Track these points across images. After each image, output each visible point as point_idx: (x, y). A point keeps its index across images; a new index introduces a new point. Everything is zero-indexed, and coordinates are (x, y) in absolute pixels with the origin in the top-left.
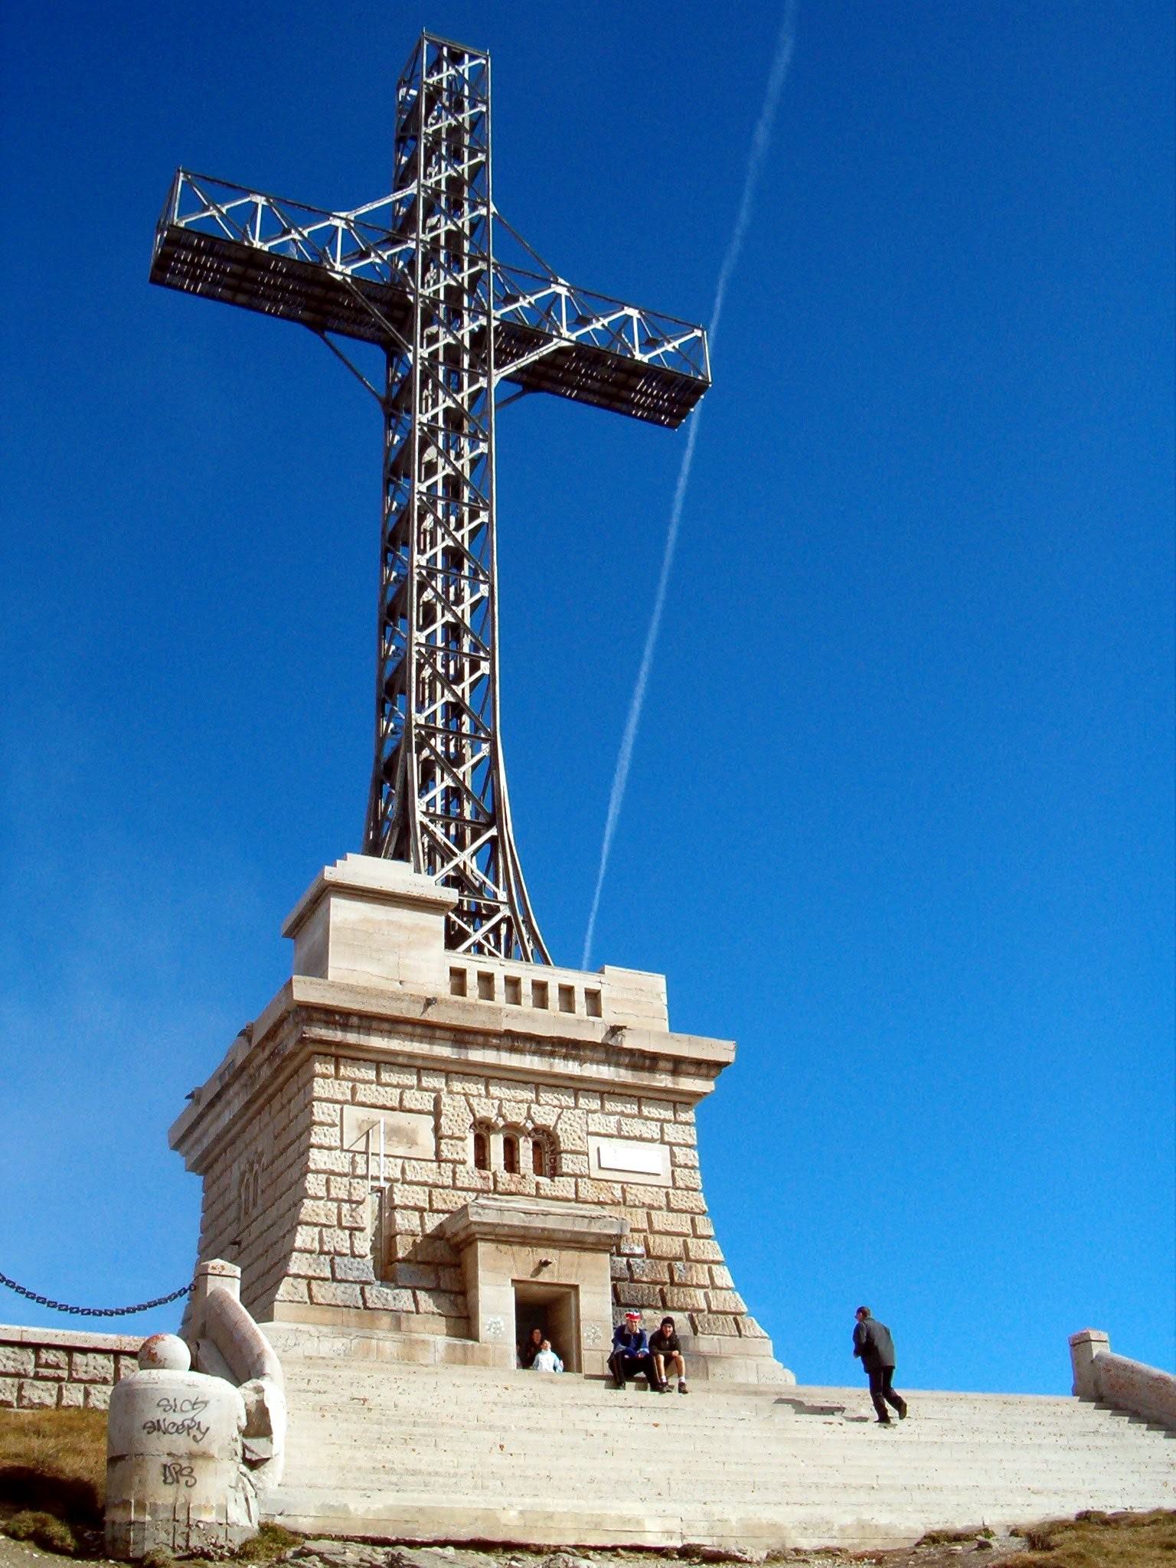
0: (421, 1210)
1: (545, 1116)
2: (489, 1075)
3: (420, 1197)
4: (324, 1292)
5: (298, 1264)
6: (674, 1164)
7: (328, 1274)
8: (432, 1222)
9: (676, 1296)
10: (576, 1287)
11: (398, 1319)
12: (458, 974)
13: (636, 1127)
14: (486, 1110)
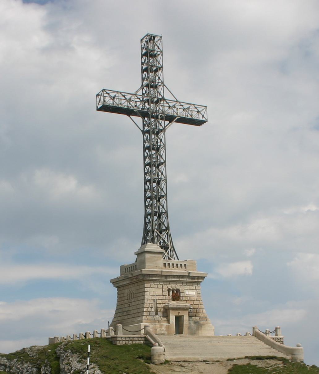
0: (161, 304)
1: (178, 287)
2: (170, 282)
3: (160, 302)
4: (149, 318)
5: (145, 314)
6: (197, 293)
7: (149, 315)
8: (162, 306)
9: (197, 315)
10: (183, 315)
11: (159, 321)
12: (165, 264)
13: (191, 287)
14: (170, 287)
